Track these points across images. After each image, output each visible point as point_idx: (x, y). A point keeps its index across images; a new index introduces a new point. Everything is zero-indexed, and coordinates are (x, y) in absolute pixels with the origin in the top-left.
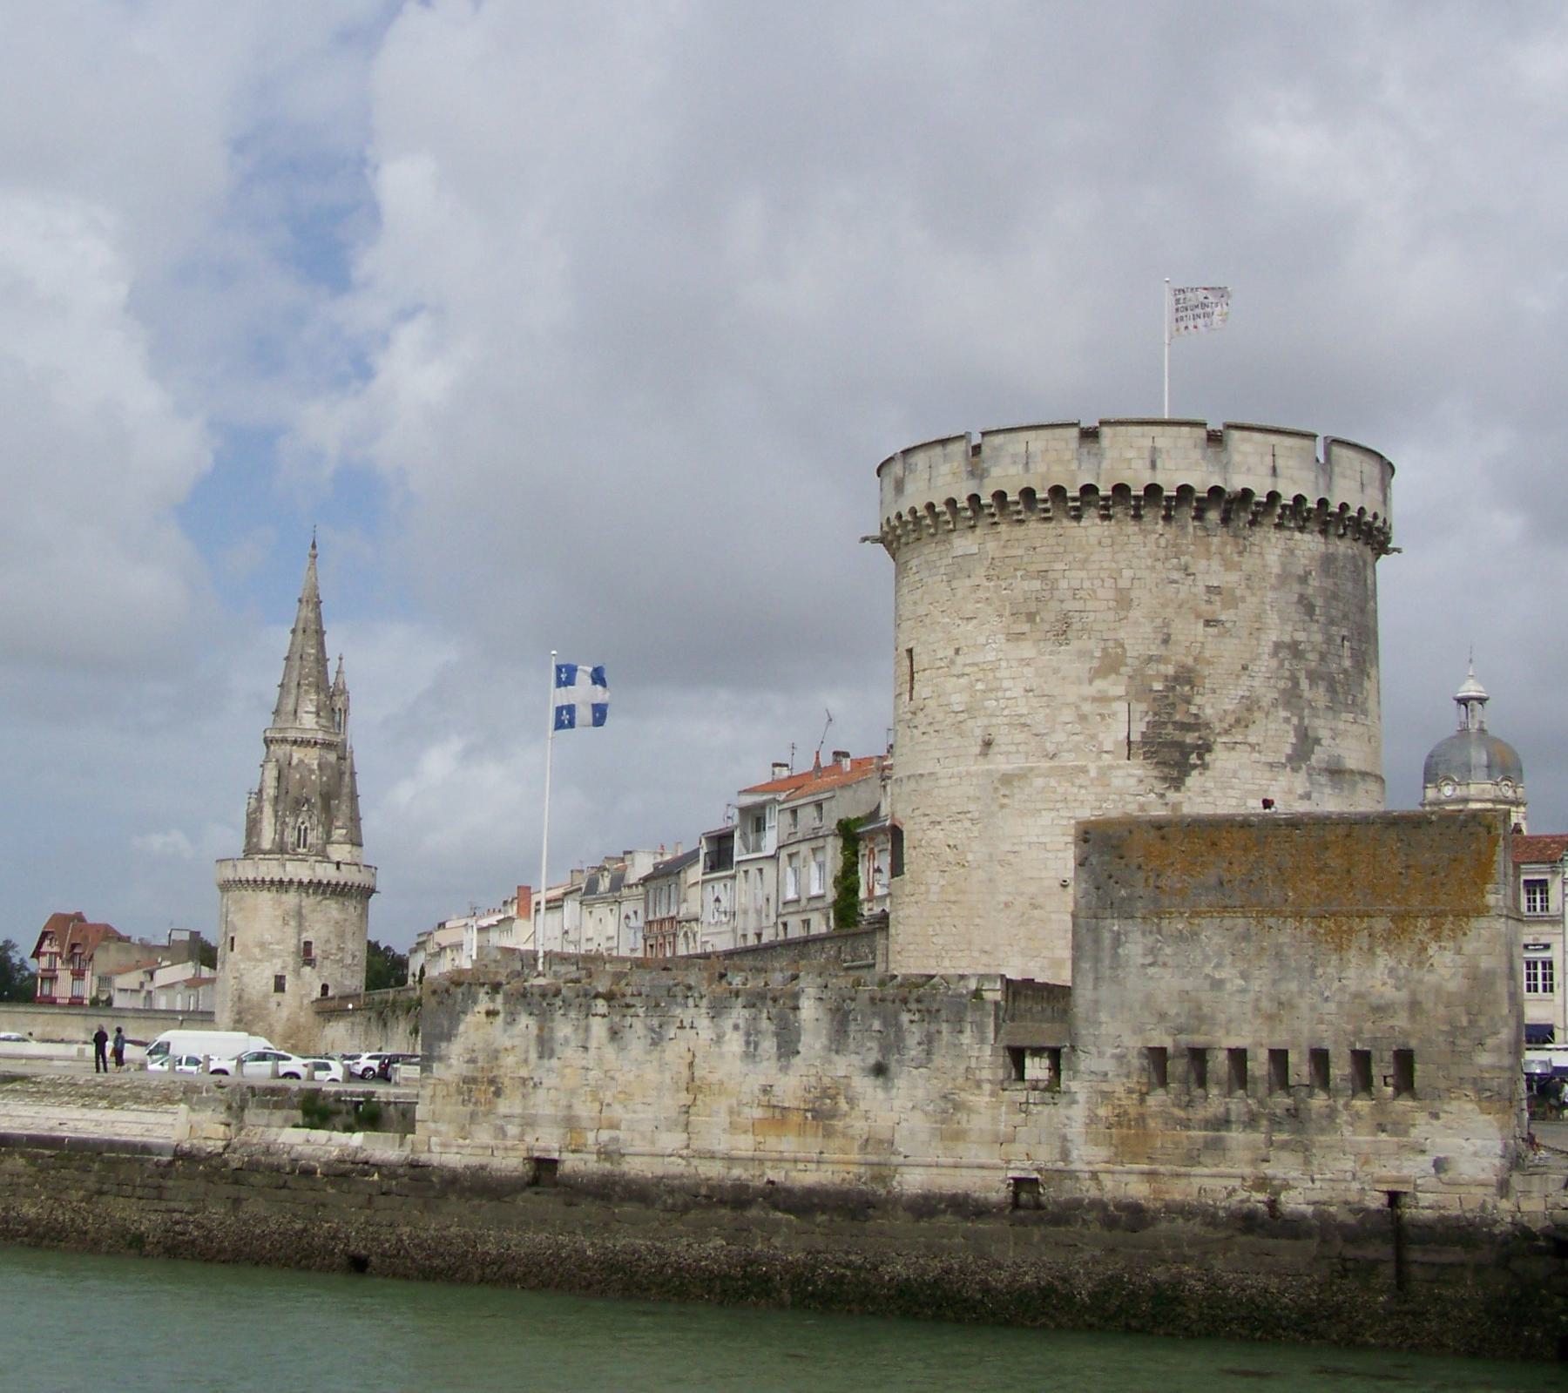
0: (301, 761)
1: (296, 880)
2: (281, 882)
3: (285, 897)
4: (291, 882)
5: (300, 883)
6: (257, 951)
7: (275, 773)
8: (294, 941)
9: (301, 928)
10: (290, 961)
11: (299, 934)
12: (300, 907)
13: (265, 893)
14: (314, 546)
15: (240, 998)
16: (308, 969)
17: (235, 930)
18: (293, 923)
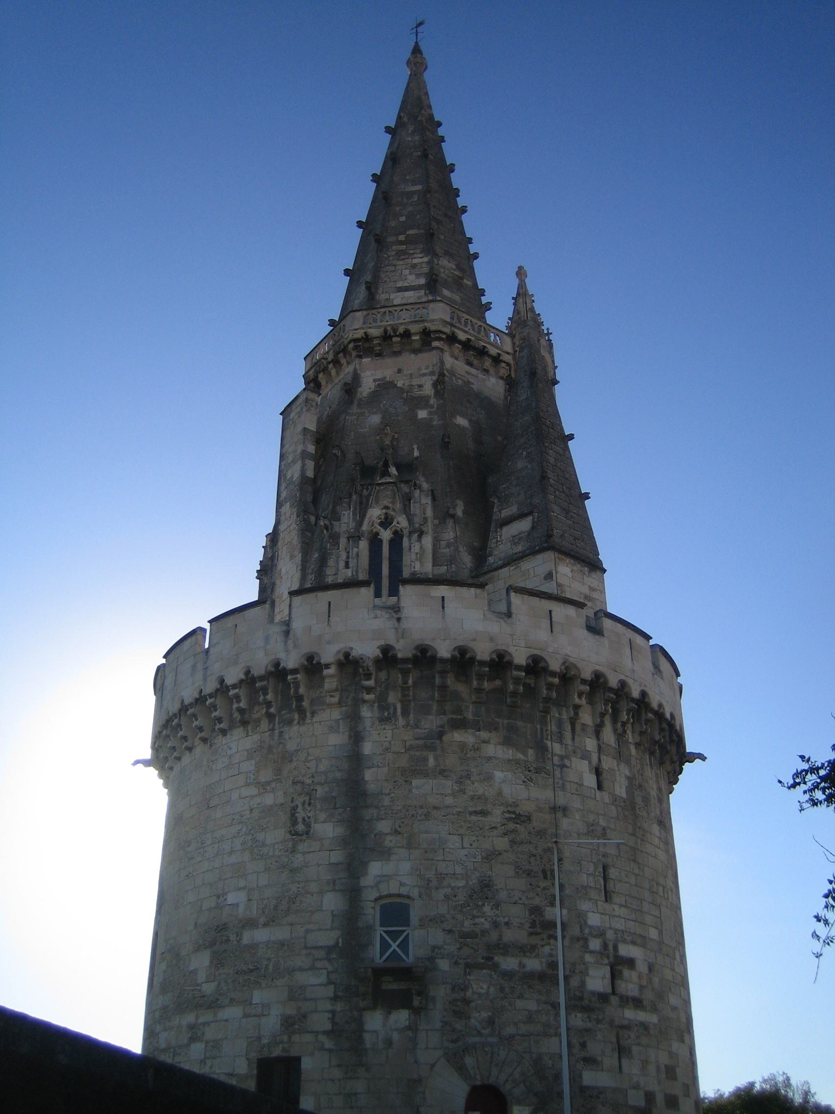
0: (385, 387)
1: (329, 654)
2: (278, 673)
3: (295, 736)
4: (313, 667)
5: (349, 663)
8: (332, 902)
9: (359, 846)
10: (315, 981)
11: (353, 868)
12: (356, 760)
16: (402, 1017)
18: (328, 830)
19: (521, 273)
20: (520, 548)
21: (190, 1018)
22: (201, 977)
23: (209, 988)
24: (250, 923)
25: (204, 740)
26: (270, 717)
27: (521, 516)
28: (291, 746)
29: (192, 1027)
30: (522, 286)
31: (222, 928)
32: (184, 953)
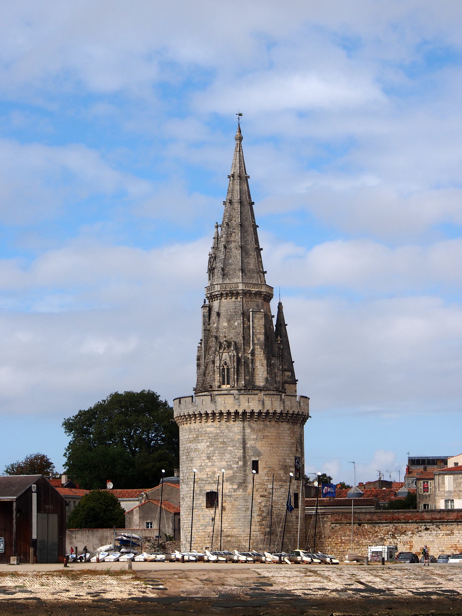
6: (282, 472)
7: (262, 322)
13: (285, 423)
14: (240, 131)
15: (271, 513)
17: (259, 454)
20: (289, 380)
21: (280, 483)
22: (282, 475)
23: (284, 478)
24: (291, 466)
25: (276, 421)
26: (292, 423)
27: (289, 371)
28: (295, 430)
29: (280, 485)
31: (286, 466)
32: (275, 469)
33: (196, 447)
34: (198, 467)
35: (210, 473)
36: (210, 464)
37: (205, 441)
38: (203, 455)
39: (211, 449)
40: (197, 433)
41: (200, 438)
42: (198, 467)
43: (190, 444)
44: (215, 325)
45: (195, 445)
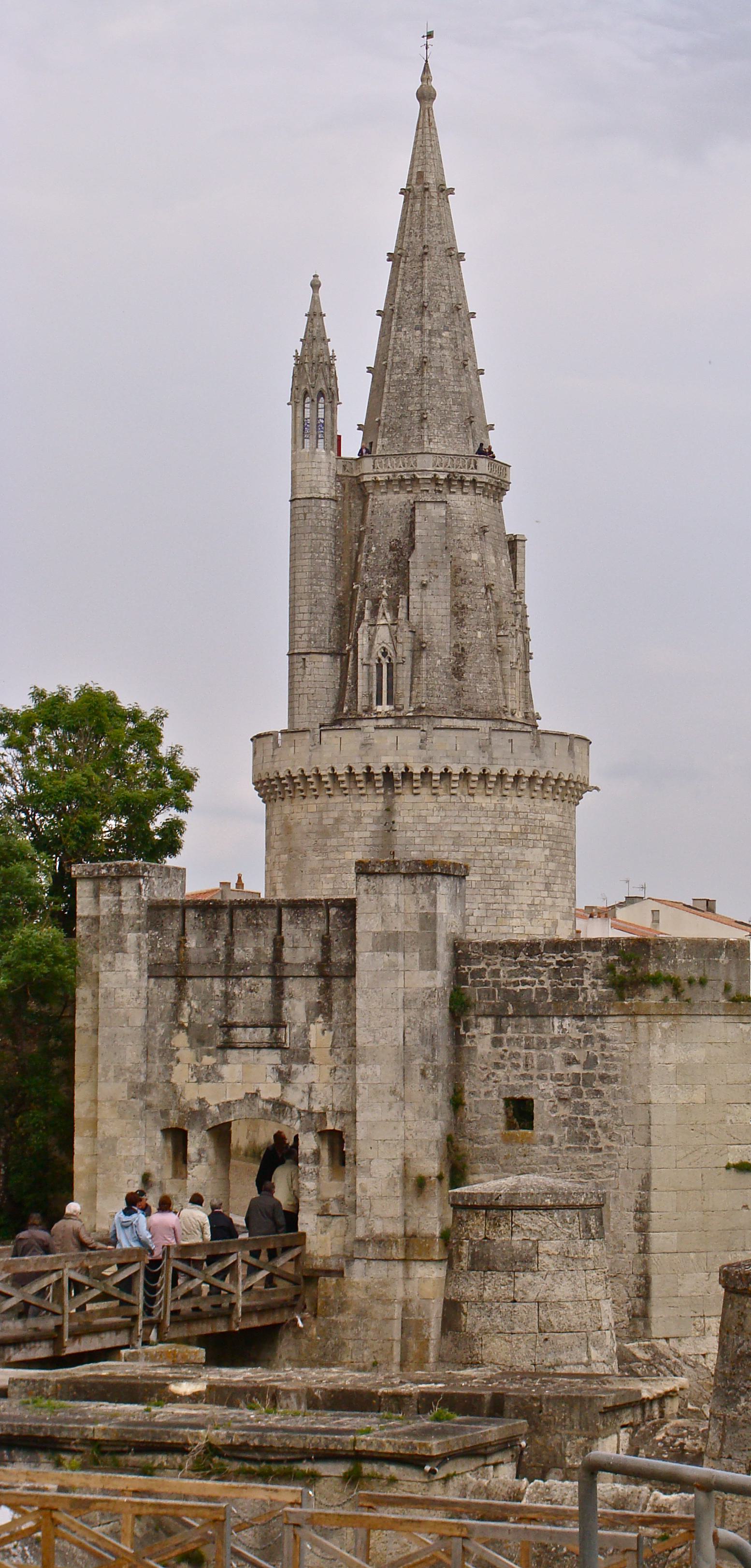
19: (315, 286)
30: (315, 302)
33: (520, 858)
34: (525, 907)
35: (549, 924)
36: (549, 901)
37: (541, 844)
38: (537, 879)
39: (552, 865)
40: (522, 822)
41: (530, 836)
42: (525, 907)
43: (500, 848)
44: (475, 557)
45: (518, 851)
